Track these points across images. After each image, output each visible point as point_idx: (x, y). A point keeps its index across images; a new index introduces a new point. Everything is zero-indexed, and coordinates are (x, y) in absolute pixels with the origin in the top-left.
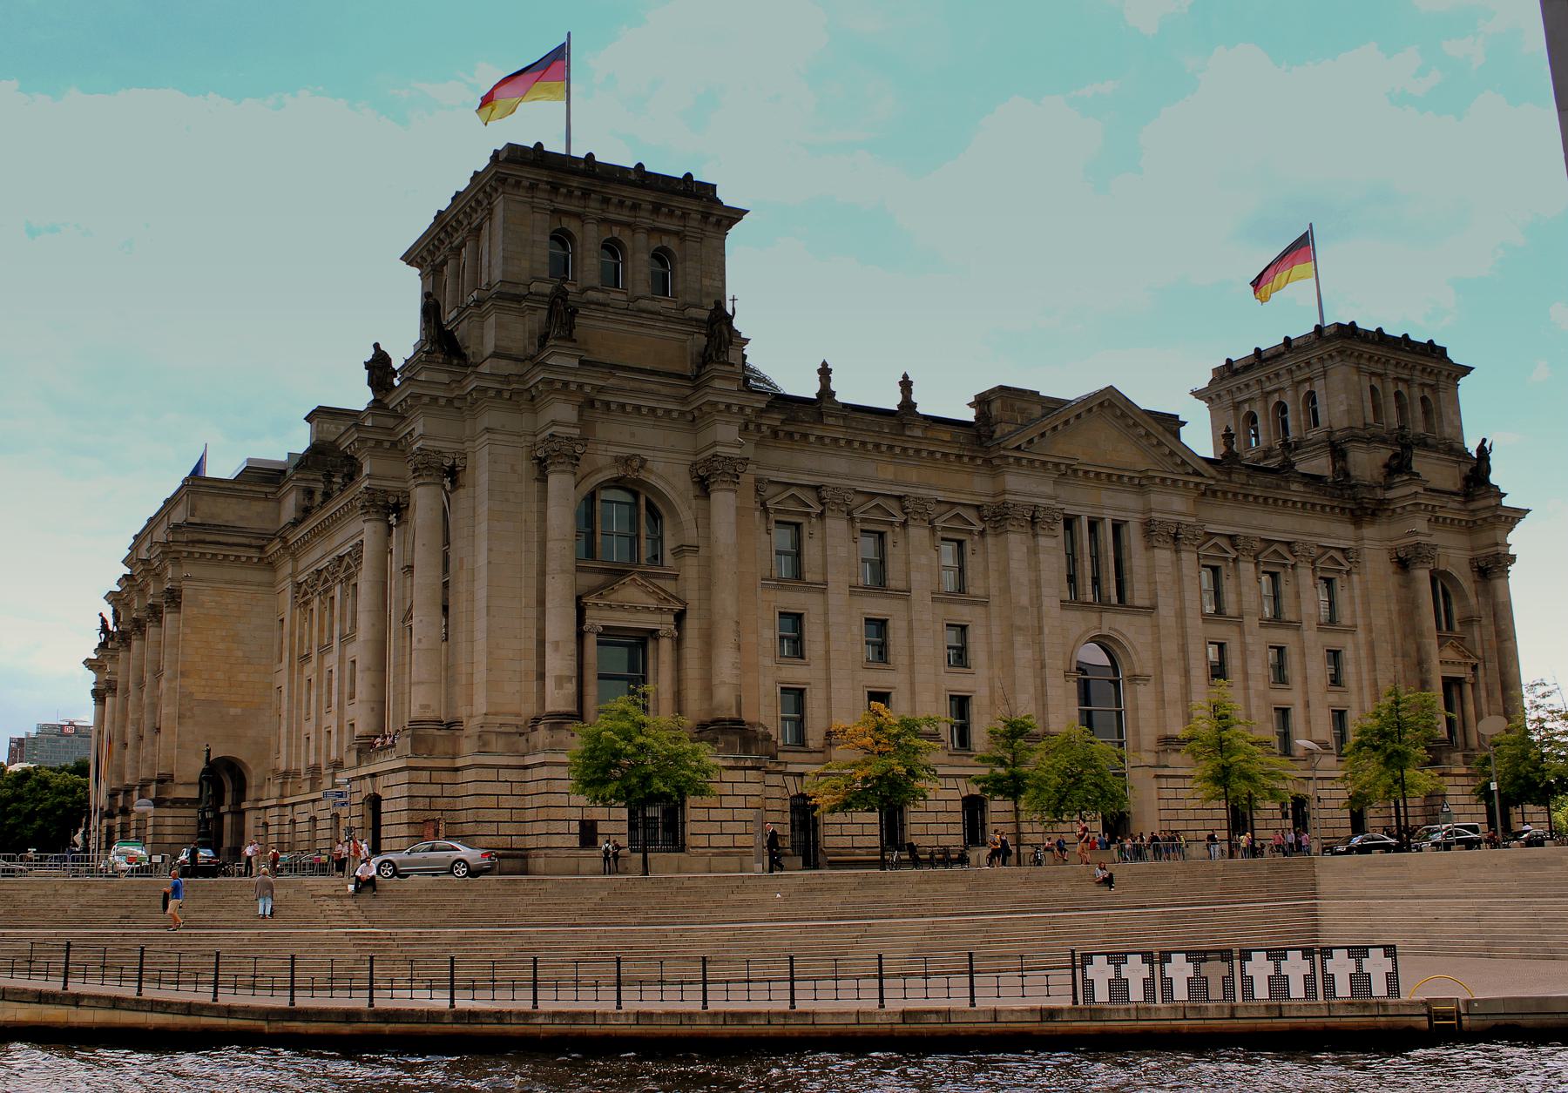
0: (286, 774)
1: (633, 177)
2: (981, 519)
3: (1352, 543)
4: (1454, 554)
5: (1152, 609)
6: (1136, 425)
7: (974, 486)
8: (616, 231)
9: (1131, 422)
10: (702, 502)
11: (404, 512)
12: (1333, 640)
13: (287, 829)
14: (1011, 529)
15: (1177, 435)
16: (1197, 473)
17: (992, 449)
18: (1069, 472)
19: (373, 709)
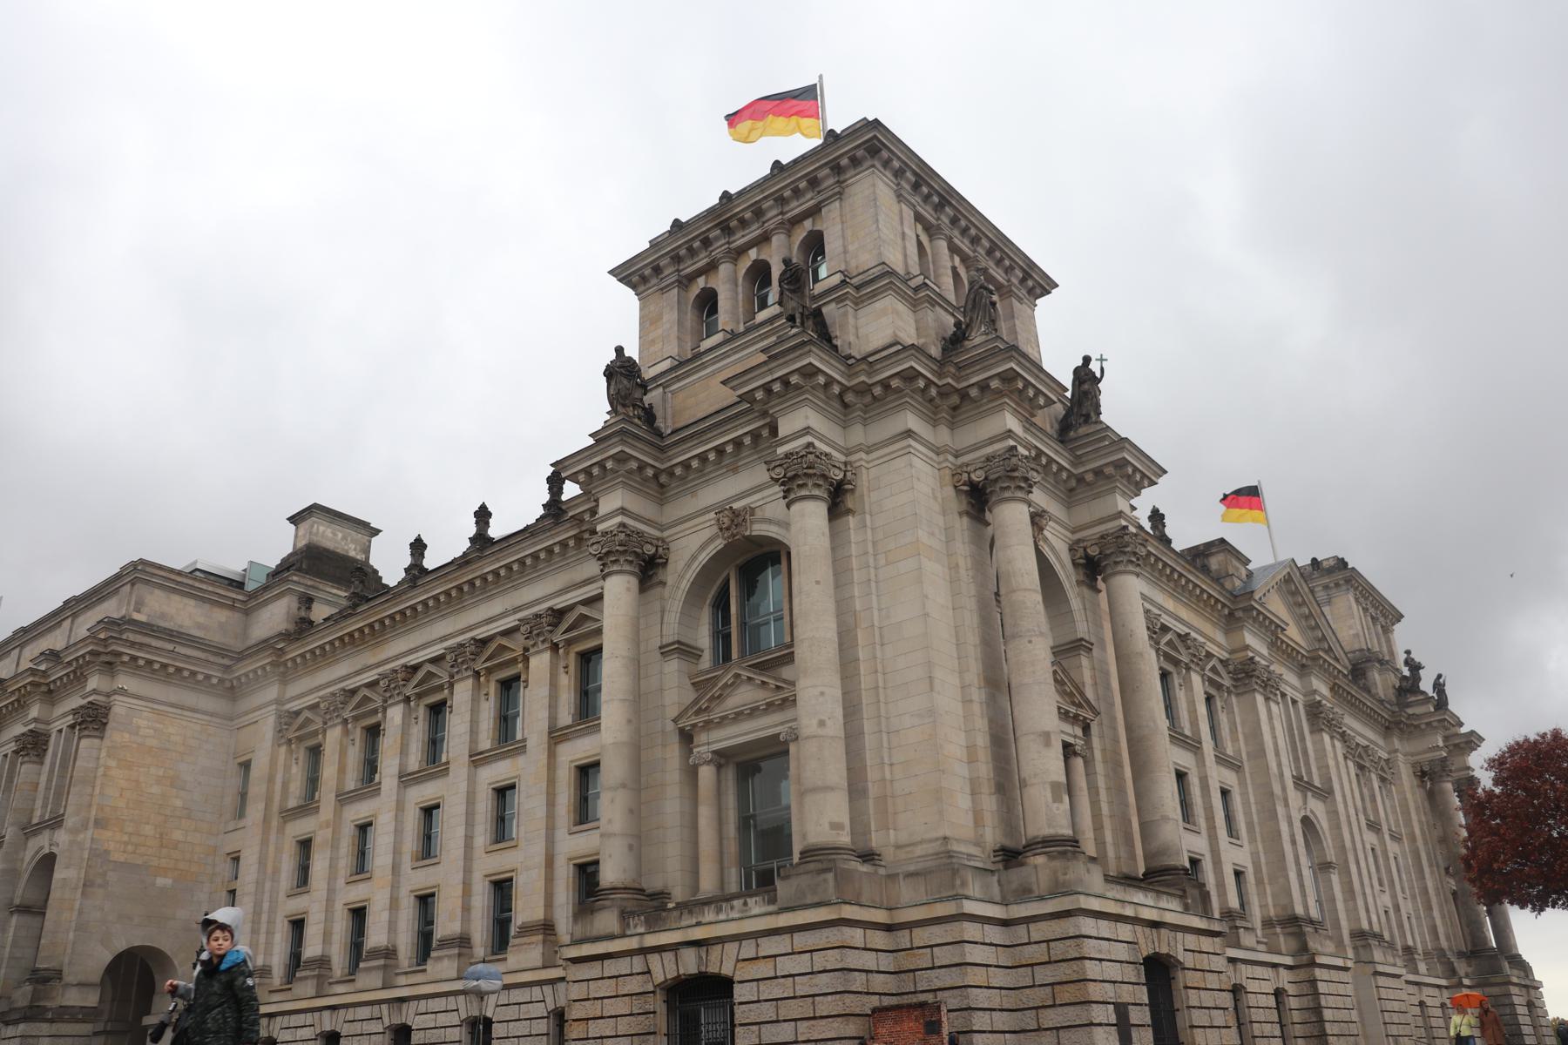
5: (1325, 793)
7: (1212, 638)
10: (1086, 591)
11: (660, 571)
14: (1256, 687)
16: (1337, 659)
17: (1238, 599)
19: (631, 847)
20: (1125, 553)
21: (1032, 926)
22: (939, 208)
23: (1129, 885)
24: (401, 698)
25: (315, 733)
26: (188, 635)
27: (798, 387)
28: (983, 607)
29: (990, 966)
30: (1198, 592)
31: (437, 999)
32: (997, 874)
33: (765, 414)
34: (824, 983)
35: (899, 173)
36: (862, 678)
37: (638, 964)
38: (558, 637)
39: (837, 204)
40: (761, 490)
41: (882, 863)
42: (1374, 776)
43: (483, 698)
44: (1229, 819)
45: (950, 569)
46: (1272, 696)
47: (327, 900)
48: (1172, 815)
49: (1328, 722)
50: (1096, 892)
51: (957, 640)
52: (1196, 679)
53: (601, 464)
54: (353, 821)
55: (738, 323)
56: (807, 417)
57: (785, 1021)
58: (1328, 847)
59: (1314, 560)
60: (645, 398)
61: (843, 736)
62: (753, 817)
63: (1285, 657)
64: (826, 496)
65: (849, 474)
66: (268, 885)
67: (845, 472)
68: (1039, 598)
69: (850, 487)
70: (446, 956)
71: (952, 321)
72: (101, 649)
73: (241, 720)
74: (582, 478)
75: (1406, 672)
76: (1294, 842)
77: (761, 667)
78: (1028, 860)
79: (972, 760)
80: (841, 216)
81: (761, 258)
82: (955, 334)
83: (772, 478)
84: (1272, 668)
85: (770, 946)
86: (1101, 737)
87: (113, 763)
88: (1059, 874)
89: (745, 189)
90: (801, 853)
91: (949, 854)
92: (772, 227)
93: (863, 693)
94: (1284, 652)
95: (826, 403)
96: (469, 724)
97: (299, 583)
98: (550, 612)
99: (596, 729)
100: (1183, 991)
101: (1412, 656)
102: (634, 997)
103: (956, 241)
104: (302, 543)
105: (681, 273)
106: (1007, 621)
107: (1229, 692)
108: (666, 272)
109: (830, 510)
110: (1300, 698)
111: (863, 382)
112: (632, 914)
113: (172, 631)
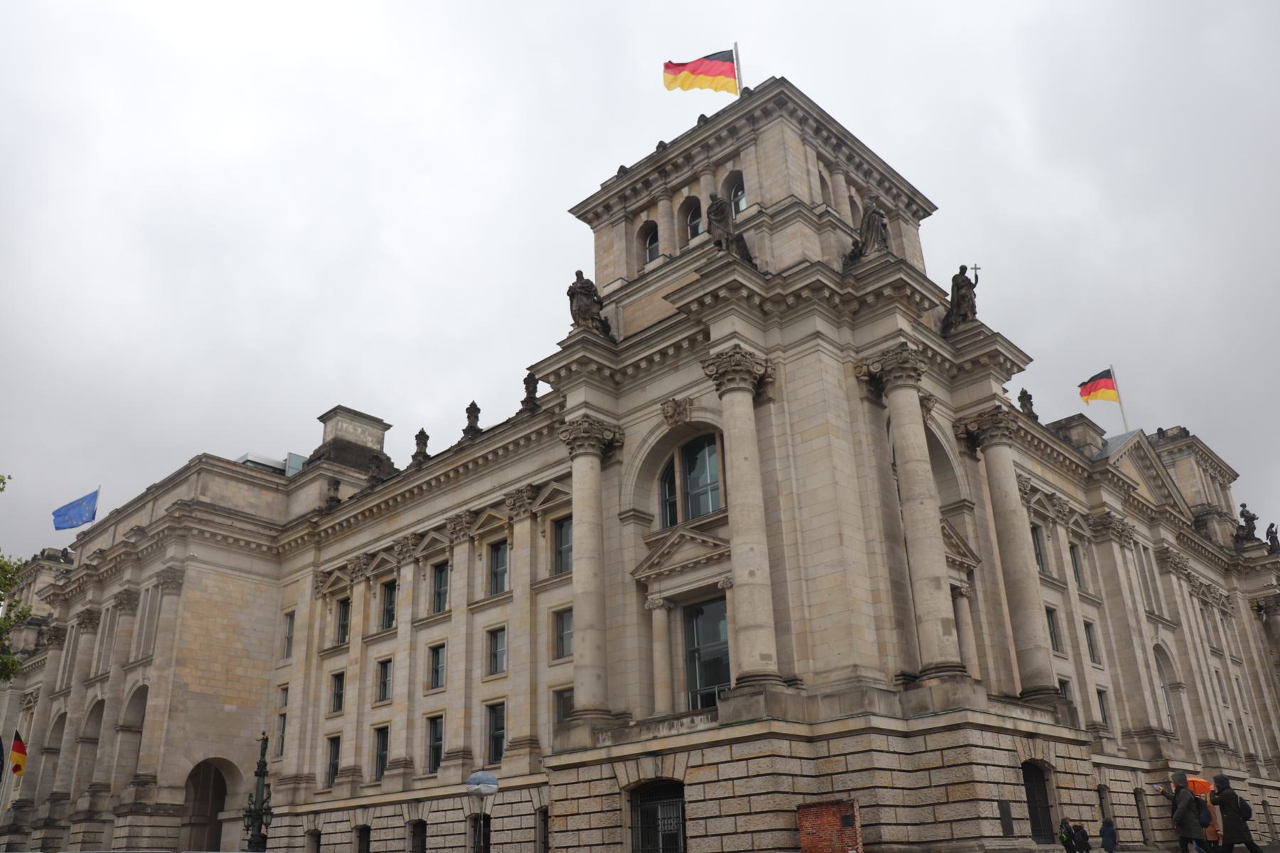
0: (297, 779)
6: (1151, 466)
7: (1074, 496)
10: (967, 460)
11: (618, 452)
13: (300, 841)
14: (1113, 537)
16: (1181, 513)
17: (1096, 464)
19: (599, 677)
20: (999, 428)
21: (928, 737)
22: (837, 148)
23: (1009, 703)
24: (412, 559)
25: (344, 589)
26: (243, 513)
27: (725, 299)
28: (882, 475)
29: (894, 770)
30: (1061, 458)
31: (446, 800)
32: (898, 695)
33: (699, 322)
34: (757, 785)
35: (803, 121)
36: (784, 536)
37: (606, 771)
38: (536, 508)
39: (753, 148)
40: (698, 384)
41: (804, 687)
42: (1216, 611)
43: (477, 558)
44: (1092, 647)
45: (854, 445)
46: (1126, 544)
47: (358, 722)
48: (1043, 645)
49: (1175, 565)
50: (982, 710)
51: (862, 503)
52: (1061, 531)
53: (567, 367)
54: (376, 659)
55: (675, 249)
56: (733, 324)
57: (726, 816)
58: (1178, 670)
59: (1160, 430)
60: (601, 312)
61: (768, 582)
62: (698, 650)
63: (1137, 511)
64: (751, 388)
65: (769, 369)
66: (311, 710)
67: (766, 367)
68: (928, 467)
69: (770, 380)
70: (453, 765)
71: (850, 241)
72: (177, 525)
73: (287, 579)
74: (552, 378)
75: (1242, 522)
76: (1148, 666)
77: (702, 529)
78: (924, 683)
79: (876, 600)
80: (757, 157)
81: (692, 195)
82: (853, 251)
83: (707, 375)
84: (1126, 521)
85: (713, 755)
86: (983, 581)
87: (188, 615)
88: (950, 695)
89: (677, 139)
90: (737, 680)
91: (859, 679)
92: (700, 169)
93: (786, 548)
94: (1135, 507)
95: (749, 312)
96: (466, 579)
97: (328, 469)
98: (529, 488)
99: (569, 581)
100: (1056, 791)
101: (1247, 509)
102: (604, 798)
103: (852, 175)
104: (329, 438)
105: (628, 210)
106: (903, 486)
107: (1090, 542)
108: (615, 209)
109: (754, 399)
110: (1150, 546)
111: (779, 293)
112: (601, 730)
113: (230, 509)
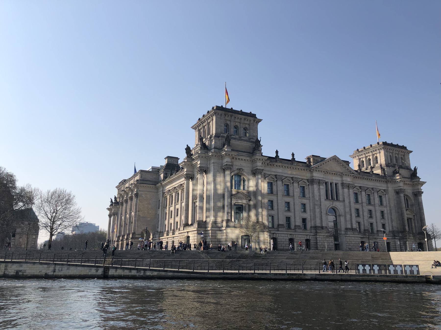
0: (160, 232)
1: (240, 113)
2: (308, 182)
3: (386, 189)
4: (409, 190)
5: (344, 201)
7: (306, 175)
8: (237, 124)
9: (339, 162)
12: (382, 209)
14: (314, 184)
15: (349, 165)
16: (353, 173)
18: (326, 173)
19: (186, 218)
110: (340, 183)
